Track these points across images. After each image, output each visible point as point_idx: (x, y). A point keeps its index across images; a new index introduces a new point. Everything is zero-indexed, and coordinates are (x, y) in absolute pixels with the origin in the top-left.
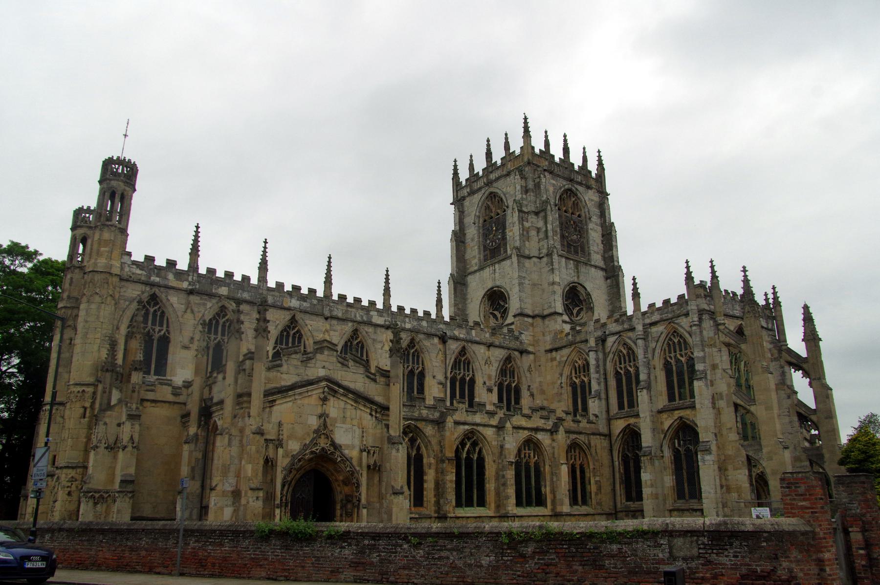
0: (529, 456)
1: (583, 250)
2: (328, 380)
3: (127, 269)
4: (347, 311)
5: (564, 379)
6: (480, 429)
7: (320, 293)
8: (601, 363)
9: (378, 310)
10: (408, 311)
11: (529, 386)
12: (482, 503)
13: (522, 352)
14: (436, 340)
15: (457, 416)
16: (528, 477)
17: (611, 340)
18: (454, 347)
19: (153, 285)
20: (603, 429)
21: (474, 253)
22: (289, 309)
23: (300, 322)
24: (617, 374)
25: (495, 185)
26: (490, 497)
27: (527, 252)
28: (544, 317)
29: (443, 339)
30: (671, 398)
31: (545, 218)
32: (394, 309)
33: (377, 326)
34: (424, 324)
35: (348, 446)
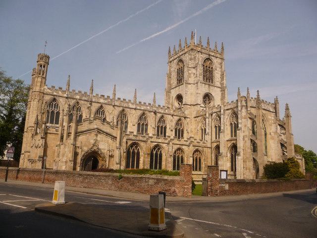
1: (212, 81)
3: (45, 91)
5: (199, 128)
7: (111, 98)
8: (210, 123)
13: (185, 118)
14: (152, 113)
15: (152, 140)
17: (214, 114)
18: (159, 115)
20: (209, 145)
21: (174, 82)
22: (100, 103)
24: (216, 126)
25: (181, 57)
27: (189, 82)
28: (194, 105)
29: (155, 113)
30: (232, 136)
31: (196, 70)
32: (138, 103)
34: (148, 108)
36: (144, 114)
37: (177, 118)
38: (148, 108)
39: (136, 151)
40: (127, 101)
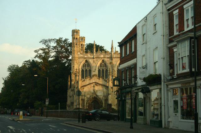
2: (95, 82)
19: (85, 58)
35: (100, 96)
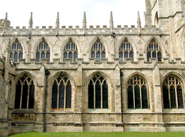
0: (138, 83)
4: (65, 32)
6: (103, 71)
7: (54, 27)
9: (80, 29)
10: (95, 27)
11: (166, 51)
12: (106, 106)
13: (161, 36)
14: (110, 37)
16: (137, 94)
18: (120, 38)
22: (41, 35)
23: (46, 39)
26: (110, 104)
29: (114, 35)
32: (88, 27)
33: (79, 35)
36: (98, 40)
37: (148, 38)
38: (104, 31)
39: (65, 84)
40: (74, 27)
